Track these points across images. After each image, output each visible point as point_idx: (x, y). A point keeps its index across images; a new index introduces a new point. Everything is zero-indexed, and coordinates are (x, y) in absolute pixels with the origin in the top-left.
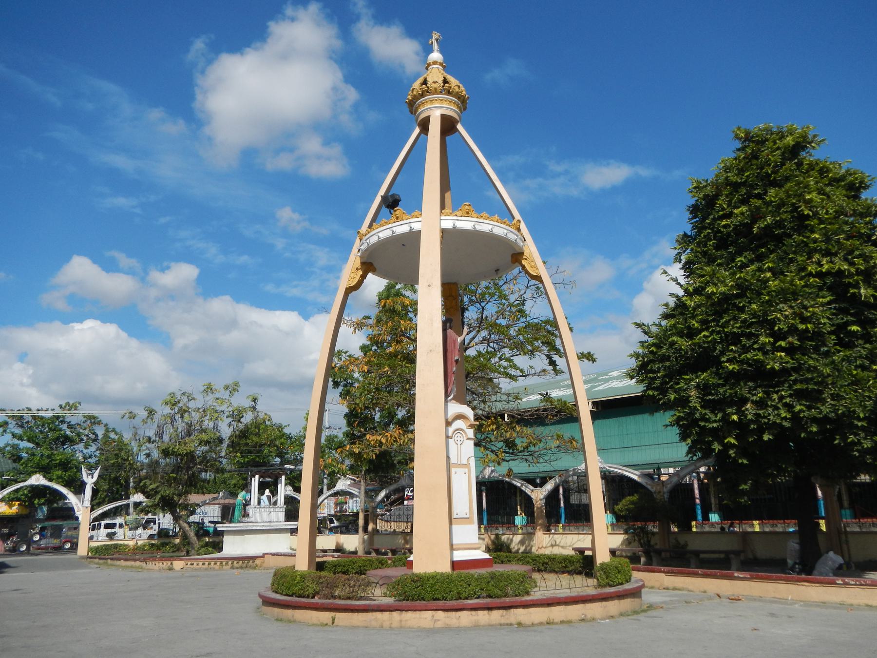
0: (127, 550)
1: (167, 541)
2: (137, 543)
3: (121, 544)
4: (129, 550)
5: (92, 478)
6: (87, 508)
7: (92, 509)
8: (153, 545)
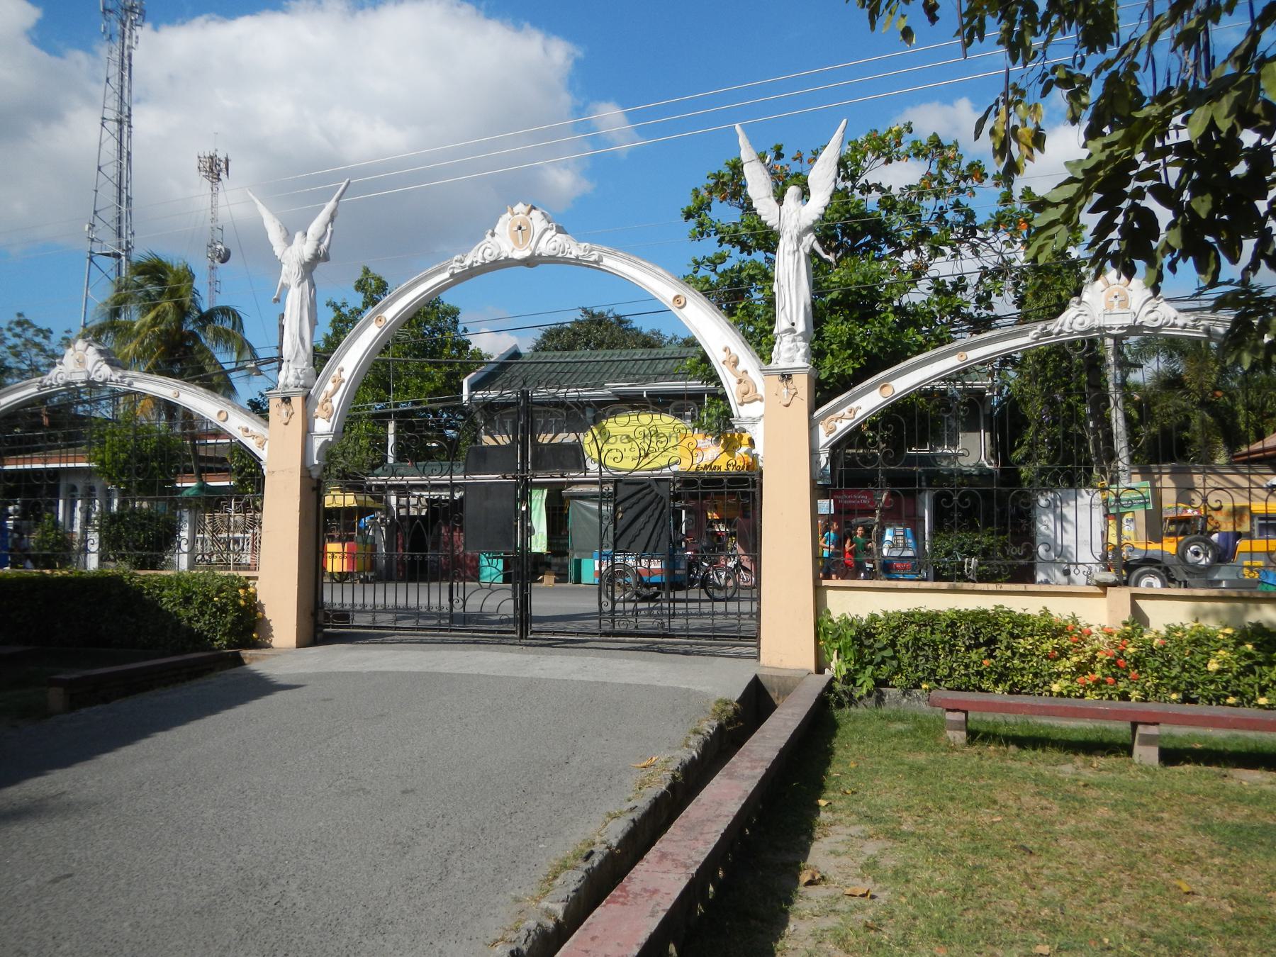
0: (1065, 665)
2: (1139, 618)
4: (1081, 669)
5: (805, 194)
6: (786, 377)
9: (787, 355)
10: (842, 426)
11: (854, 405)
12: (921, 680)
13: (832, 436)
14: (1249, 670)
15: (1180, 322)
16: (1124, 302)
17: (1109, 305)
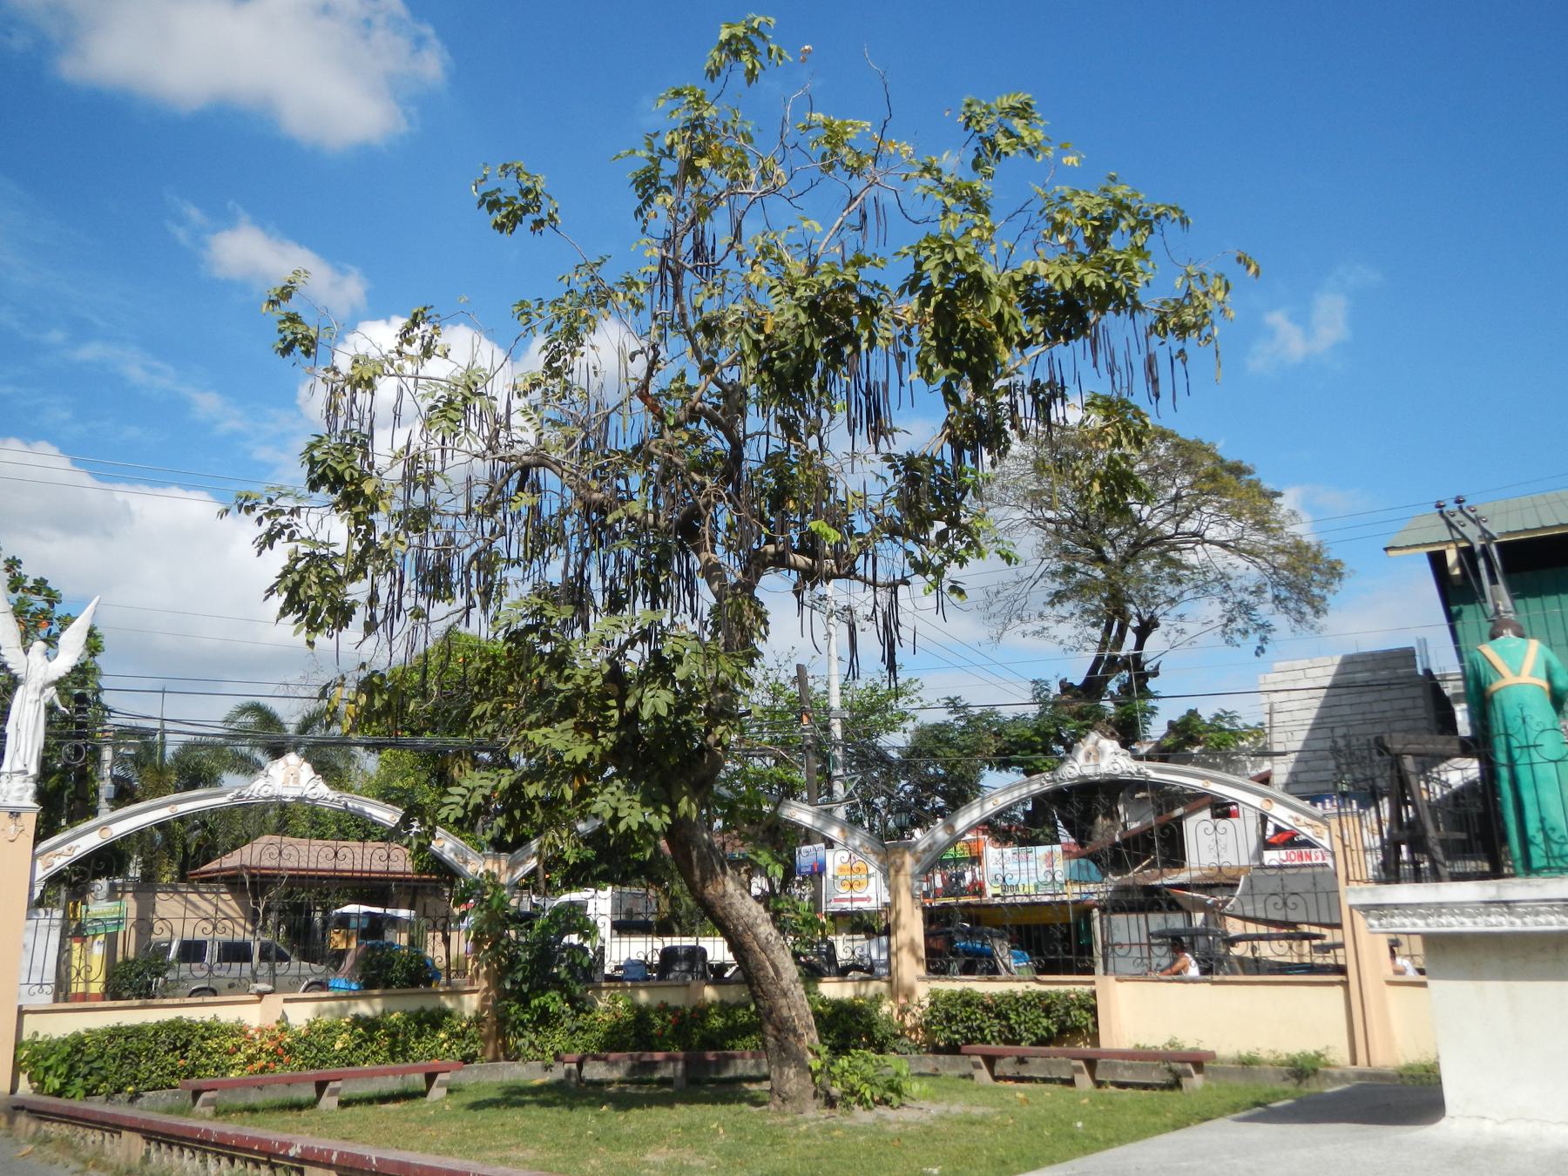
0: (240, 1058)
1: (429, 1004)
3: (208, 1027)
4: (251, 1060)
6: (15, 814)
7: (46, 829)
8: (369, 1025)
9: (17, 794)
10: (60, 861)
11: (74, 844)
12: (124, 1084)
13: (48, 870)
14: (359, 1046)
15: (330, 797)
16: (297, 780)
17: (287, 780)
